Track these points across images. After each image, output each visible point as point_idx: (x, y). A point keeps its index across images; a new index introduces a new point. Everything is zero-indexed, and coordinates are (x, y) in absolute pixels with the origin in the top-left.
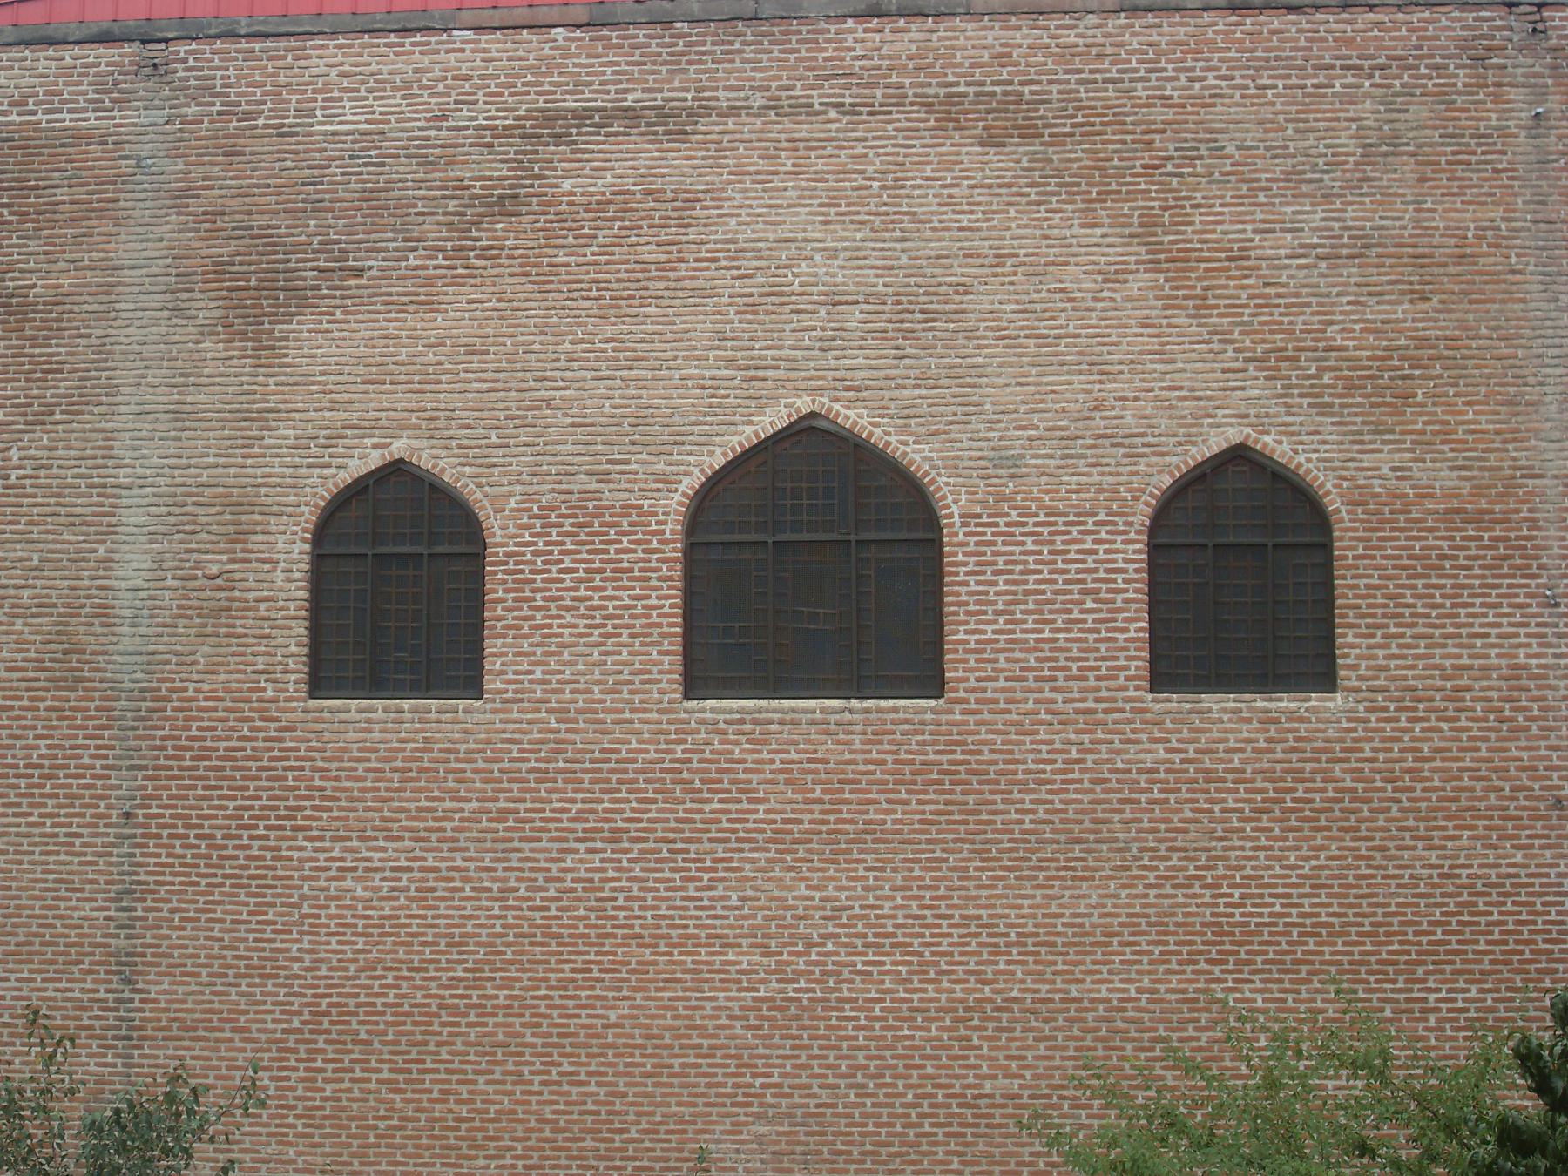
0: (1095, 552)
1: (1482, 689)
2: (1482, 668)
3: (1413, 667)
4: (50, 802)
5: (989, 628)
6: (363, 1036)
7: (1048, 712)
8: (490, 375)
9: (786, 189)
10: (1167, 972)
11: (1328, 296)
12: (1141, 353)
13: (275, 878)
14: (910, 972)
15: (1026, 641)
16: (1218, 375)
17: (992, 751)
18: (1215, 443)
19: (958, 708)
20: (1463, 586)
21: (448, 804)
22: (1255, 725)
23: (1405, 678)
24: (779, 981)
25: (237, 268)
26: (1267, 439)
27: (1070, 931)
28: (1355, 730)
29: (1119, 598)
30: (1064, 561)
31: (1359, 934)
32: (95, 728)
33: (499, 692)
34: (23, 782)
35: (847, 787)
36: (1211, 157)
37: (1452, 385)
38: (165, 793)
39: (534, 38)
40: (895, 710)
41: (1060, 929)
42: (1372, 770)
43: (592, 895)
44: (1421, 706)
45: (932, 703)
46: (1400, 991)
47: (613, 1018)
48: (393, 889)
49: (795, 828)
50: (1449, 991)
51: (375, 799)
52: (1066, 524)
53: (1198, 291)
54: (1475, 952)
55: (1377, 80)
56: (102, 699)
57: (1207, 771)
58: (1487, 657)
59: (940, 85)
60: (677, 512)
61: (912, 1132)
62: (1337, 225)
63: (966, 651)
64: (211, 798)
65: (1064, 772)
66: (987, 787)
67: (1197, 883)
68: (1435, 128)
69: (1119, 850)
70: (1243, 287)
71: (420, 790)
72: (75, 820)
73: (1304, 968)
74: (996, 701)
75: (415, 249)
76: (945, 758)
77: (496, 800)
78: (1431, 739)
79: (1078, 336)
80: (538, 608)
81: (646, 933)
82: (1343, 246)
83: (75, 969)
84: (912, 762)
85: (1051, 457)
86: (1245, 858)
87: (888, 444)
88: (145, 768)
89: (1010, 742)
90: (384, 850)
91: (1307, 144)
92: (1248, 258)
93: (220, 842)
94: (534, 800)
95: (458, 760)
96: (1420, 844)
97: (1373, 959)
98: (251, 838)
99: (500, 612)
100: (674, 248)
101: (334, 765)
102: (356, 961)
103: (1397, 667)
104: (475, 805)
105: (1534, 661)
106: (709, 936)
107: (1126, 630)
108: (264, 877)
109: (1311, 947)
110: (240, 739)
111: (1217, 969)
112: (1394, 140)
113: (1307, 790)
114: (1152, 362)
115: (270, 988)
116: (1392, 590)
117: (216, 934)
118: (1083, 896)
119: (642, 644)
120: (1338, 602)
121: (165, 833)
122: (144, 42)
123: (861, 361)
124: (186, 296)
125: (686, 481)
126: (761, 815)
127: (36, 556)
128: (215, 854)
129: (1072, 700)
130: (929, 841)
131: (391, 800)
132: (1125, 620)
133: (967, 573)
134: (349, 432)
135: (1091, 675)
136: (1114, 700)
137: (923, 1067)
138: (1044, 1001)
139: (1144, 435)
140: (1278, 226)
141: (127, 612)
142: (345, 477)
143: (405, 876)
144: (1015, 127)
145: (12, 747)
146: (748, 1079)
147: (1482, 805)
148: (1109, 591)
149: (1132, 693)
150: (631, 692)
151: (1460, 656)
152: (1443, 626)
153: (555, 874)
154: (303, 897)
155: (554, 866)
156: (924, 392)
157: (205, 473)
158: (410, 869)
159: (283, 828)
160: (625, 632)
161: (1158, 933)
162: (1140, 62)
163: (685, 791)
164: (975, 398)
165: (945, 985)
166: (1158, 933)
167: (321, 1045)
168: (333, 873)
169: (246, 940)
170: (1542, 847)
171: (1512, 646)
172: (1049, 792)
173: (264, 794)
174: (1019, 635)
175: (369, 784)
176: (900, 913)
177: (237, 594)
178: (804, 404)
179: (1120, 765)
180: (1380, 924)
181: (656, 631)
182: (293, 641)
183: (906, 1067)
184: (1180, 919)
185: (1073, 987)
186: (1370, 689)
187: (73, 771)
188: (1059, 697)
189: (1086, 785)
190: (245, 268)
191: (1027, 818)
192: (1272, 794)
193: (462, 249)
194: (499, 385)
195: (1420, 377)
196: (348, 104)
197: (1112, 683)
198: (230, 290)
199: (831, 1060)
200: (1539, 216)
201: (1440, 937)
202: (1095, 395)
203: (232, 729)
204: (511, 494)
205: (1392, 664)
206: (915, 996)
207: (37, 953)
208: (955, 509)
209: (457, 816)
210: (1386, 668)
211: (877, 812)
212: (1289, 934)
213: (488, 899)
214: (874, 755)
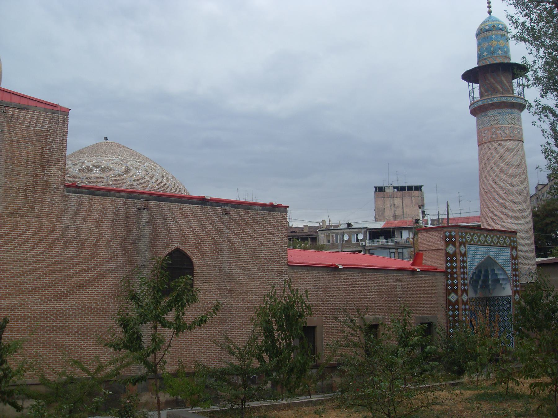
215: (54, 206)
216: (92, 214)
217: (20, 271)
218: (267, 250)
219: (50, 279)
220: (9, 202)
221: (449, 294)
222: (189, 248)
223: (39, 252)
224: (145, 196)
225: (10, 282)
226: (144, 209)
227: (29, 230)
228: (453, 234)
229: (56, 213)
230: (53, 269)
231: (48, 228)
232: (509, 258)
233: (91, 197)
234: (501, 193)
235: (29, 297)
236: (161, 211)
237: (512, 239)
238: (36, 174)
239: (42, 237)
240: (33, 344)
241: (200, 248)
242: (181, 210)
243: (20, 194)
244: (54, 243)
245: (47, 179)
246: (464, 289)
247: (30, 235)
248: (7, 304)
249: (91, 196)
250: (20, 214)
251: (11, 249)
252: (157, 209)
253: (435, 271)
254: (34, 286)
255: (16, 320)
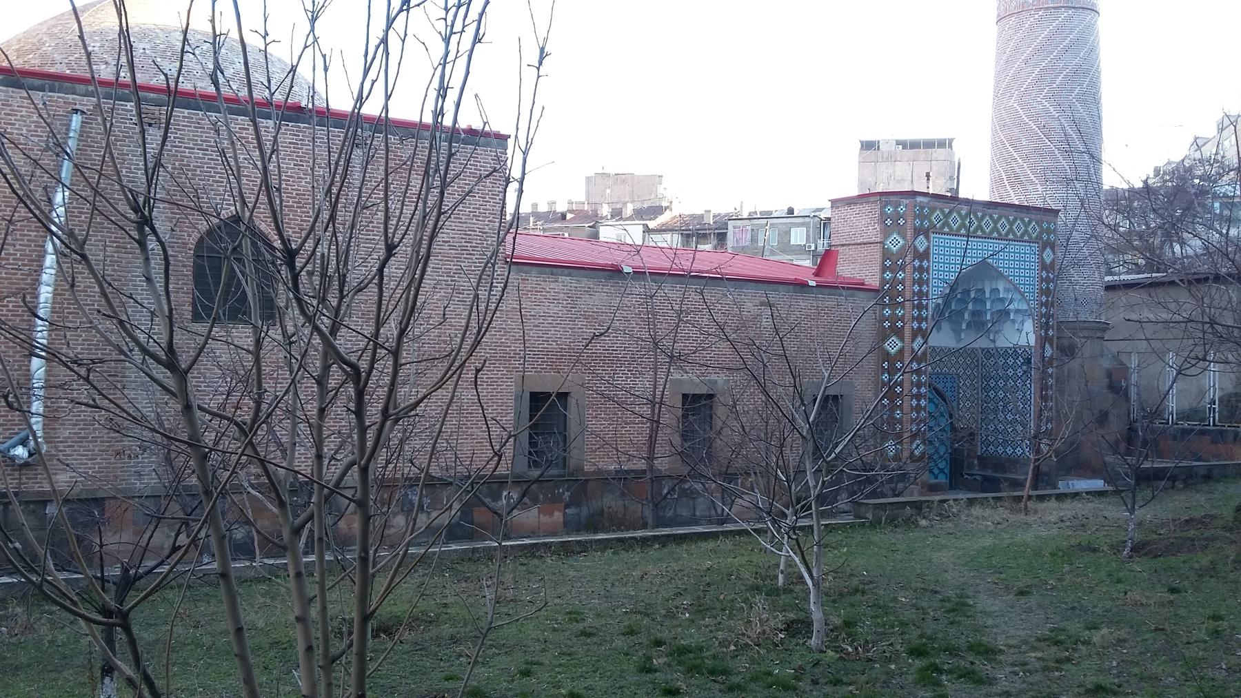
216: (16, 131)
218: (456, 228)
221: (885, 338)
222: (264, 217)
224: (152, 95)
226: (150, 125)
228: (902, 209)
232: (1036, 266)
233: (13, 92)
234: (1034, 127)
236: (193, 131)
237: (1045, 225)
241: (291, 216)
242: (245, 132)
246: (920, 328)
249: (11, 89)
252: (183, 126)
253: (858, 287)
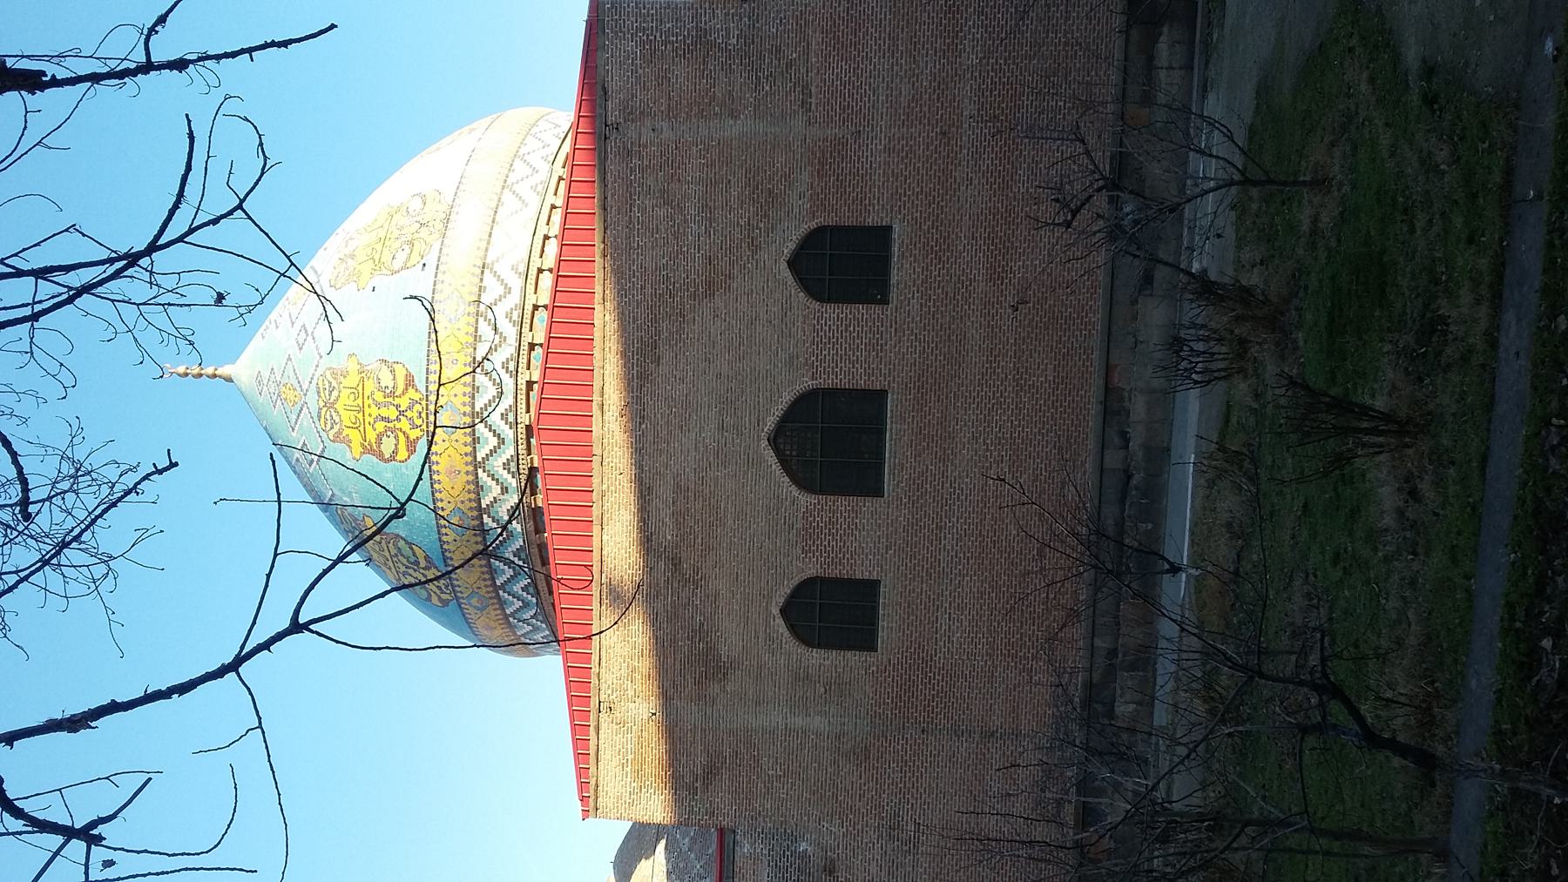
0: (830, 325)
1: (893, 165)
2: (885, 163)
3: (883, 194)
4: (916, 763)
5: (860, 371)
6: (1019, 636)
7: (895, 347)
8: (747, 571)
9: (674, 447)
10: (1005, 301)
11: (726, 223)
12: (748, 303)
13: (951, 670)
14: (1001, 409)
15: (866, 356)
16: (758, 271)
17: (911, 371)
18: (786, 273)
19: (892, 385)
20: (850, 171)
21: (923, 596)
22: (904, 262)
23: (887, 198)
24: (1002, 463)
25: (697, 676)
26: (785, 251)
27: (987, 342)
28: (908, 220)
29: (849, 316)
30: (833, 338)
31: (994, 221)
32: (886, 742)
33: (878, 574)
34: (908, 775)
35: (923, 431)
36: (667, 269)
37: (766, 172)
38: (915, 714)
39: (606, 549)
40: (892, 411)
41: (985, 346)
42: (925, 212)
43: (963, 538)
44: (899, 191)
45: (889, 395)
46: (1019, 204)
47: (1015, 532)
48: (958, 620)
49: (939, 454)
50: (1020, 182)
51: (920, 627)
52: (818, 337)
53: (723, 277)
54: (1004, 171)
55: (636, 198)
56: (874, 739)
57: (922, 282)
58: (880, 162)
59: (633, 381)
60: (807, 498)
61: (1068, 411)
62: (697, 218)
63: (869, 380)
64: (917, 695)
65: (920, 342)
66: (925, 374)
67: (969, 288)
68: (657, 174)
69: (954, 320)
70: (722, 258)
71: (917, 607)
72: (925, 753)
73: (1006, 244)
74: (890, 369)
75: (693, 601)
76: (912, 391)
77: (922, 577)
78: (913, 188)
79: (740, 329)
80: (844, 556)
81: (980, 517)
82: (706, 214)
83: (987, 756)
84: (913, 405)
85: (790, 342)
86: (959, 267)
87: (782, 409)
88: (904, 722)
89: (907, 363)
90: (941, 624)
91: (663, 230)
92: (710, 256)
93: (935, 692)
94: (923, 561)
95: (905, 592)
96: (957, 193)
97: (1004, 215)
98: (934, 679)
99: (845, 572)
100: (697, 494)
101: (906, 643)
102: (987, 638)
103: (883, 200)
104: (924, 585)
105: (883, 142)
106: (982, 491)
107: (863, 314)
108: (951, 675)
109: (998, 241)
110: (893, 682)
111: (1005, 281)
112: (663, 192)
113: (932, 241)
114: (752, 298)
115: (997, 674)
116: (851, 201)
117: (974, 696)
118: (972, 335)
119: (861, 514)
120: (855, 224)
121: (931, 715)
122: (600, 712)
123: (747, 419)
124: (708, 696)
125: (794, 493)
126: (933, 468)
127: (814, 765)
128: (940, 695)
129: (891, 337)
130: (947, 399)
131: (920, 620)
132: (859, 314)
133: (837, 379)
134: (768, 631)
135: (881, 329)
136: (891, 320)
137: (1041, 405)
138: (1015, 354)
139: (782, 303)
140: (697, 243)
141: (839, 728)
142: (787, 633)
143: (952, 616)
144: (652, 350)
145: (893, 778)
146: (1043, 477)
147: (942, 167)
148: (846, 320)
149: (889, 312)
150: (880, 519)
151: (880, 174)
152: (866, 181)
153: (954, 554)
154: (960, 659)
155: (951, 554)
156: (761, 393)
157: (782, 692)
158: (950, 613)
159: (931, 665)
160: (855, 521)
161: (989, 305)
162: (626, 297)
163: (922, 499)
164: (765, 372)
165: (1006, 394)
166: (989, 305)
167: (1022, 654)
168: (950, 645)
169: (977, 683)
170: (961, 141)
171: (876, 152)
172: (928, 349)
173: (916, 673)
174: (863, 359)
175: (914, 630)
176: (976, 412)
177: (833, 681)
178: (764, 443)
179: (919, 318)
180: (990, 212)
181: (855, 508)
182: (853, 658)
183: (1040, 412)
184: (984, 296)
185: (1010, 341)
186: (891, 212)
187: (904, 753)
188: (889, 343)
189: (926, 333)
190: (697, 672)
191: (939, 358)
192: (933, 256)
193: (694, 582)
194: (751, 569)
195: (762, 185)
196: (630, 628)
197: (885, 320)
198: (706, 679)
199: (1036, 443)
200: (696, 131)
201: (997, 186)
202: (765, 323)
203: (889, 685)
204: (796, 565)
205: (881, 202)
206: (1011, 407)
207: (980, 772)
208: (810, 383)
209: (928, 593)
210: (883, 205)
211: (933, 420)
212: (992, 250)
213: (963, 581)
214: (910, 420)
215: (784, 21)
217: (909, 83)
219: (925, 22)
220: (783, 110)
223: (874, 47)
225: (930, 100)
227: (833, 67)
229: (797, 16)
230: (906, 17)
231: (827, 30)
235: (960, 62)
238: (726, 58)
239: (845, 42)
240: (1048, 52)
243: (768, 88)
244: (856, 17)
245: (733, 37)
247: (842, 66)
248: (970, 104)
250: (803, 86)
251: (869, 102)
254: (938, 54)
255: (1001, 87)
